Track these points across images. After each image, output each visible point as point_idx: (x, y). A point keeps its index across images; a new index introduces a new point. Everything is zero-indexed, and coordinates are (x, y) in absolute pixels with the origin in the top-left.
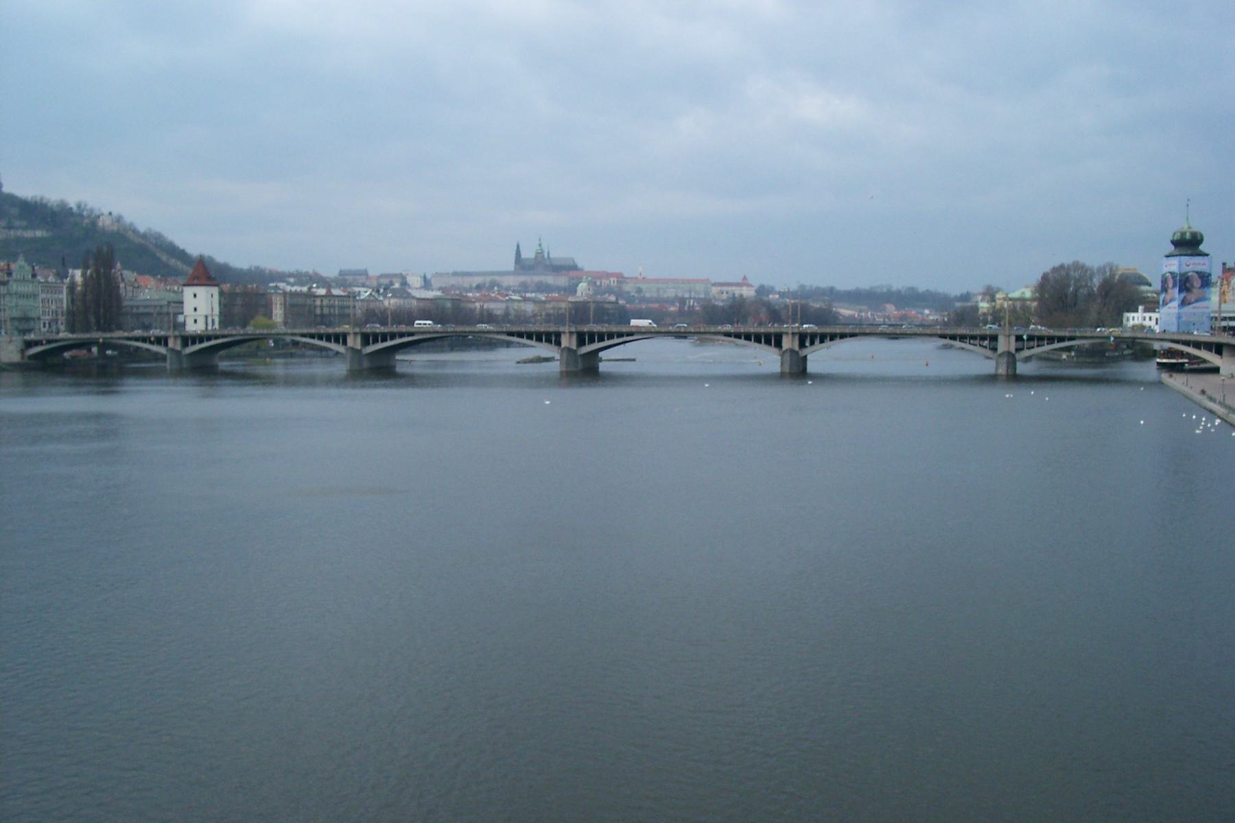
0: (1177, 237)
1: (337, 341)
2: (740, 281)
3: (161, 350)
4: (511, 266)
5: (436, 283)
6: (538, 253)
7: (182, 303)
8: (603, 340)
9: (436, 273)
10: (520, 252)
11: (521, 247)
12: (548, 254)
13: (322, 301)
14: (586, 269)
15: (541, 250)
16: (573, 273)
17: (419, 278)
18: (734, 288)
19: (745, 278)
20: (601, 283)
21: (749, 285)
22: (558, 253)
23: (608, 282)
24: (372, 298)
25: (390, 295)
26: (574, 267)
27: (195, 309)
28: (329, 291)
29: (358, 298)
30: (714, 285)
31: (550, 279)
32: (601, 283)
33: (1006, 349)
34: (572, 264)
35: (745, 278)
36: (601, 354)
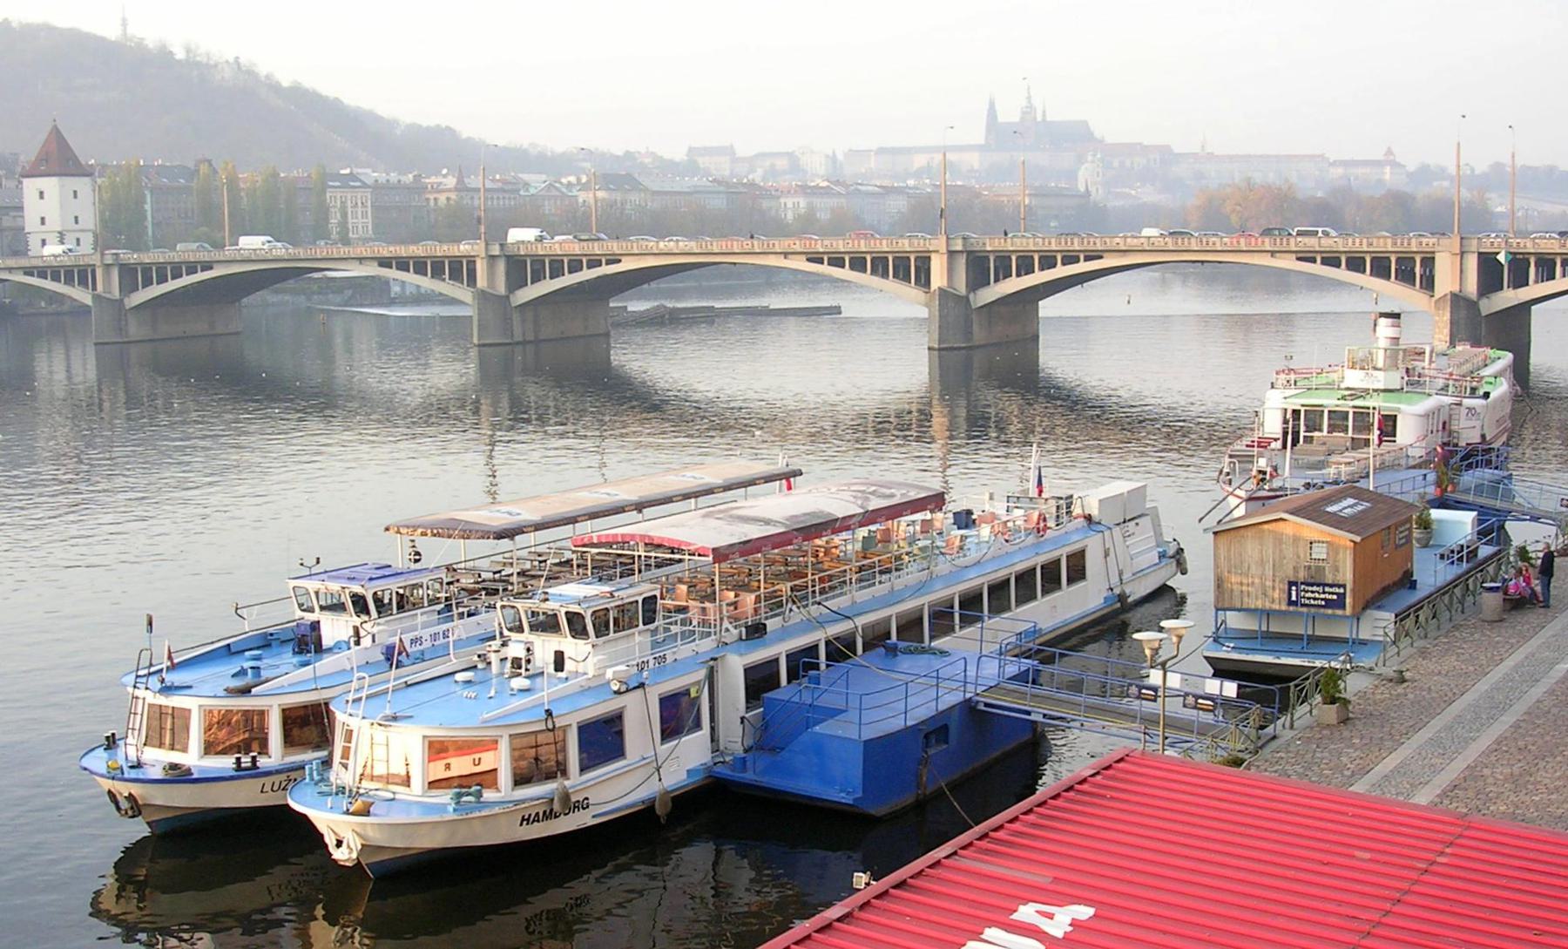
2: (1379, 155)
3: (83, 296)
4: (979, 137)
7: (21, 208)
9: (850, 150)
10: (995, 111)
11: (998, 107)
12: (1044, 112)
14: (1109, 140)
15: (1031, 107)
19: (1389, 152)
20: (1132, 163)
21: (1395, 165)
22: (1059, 111)
27: (43, 221)
28: (460, 181)
29: (522, 193)
30: (1334, 164)
32: (1132, 163)
33: (1456, 289)
35: (1389, 152)
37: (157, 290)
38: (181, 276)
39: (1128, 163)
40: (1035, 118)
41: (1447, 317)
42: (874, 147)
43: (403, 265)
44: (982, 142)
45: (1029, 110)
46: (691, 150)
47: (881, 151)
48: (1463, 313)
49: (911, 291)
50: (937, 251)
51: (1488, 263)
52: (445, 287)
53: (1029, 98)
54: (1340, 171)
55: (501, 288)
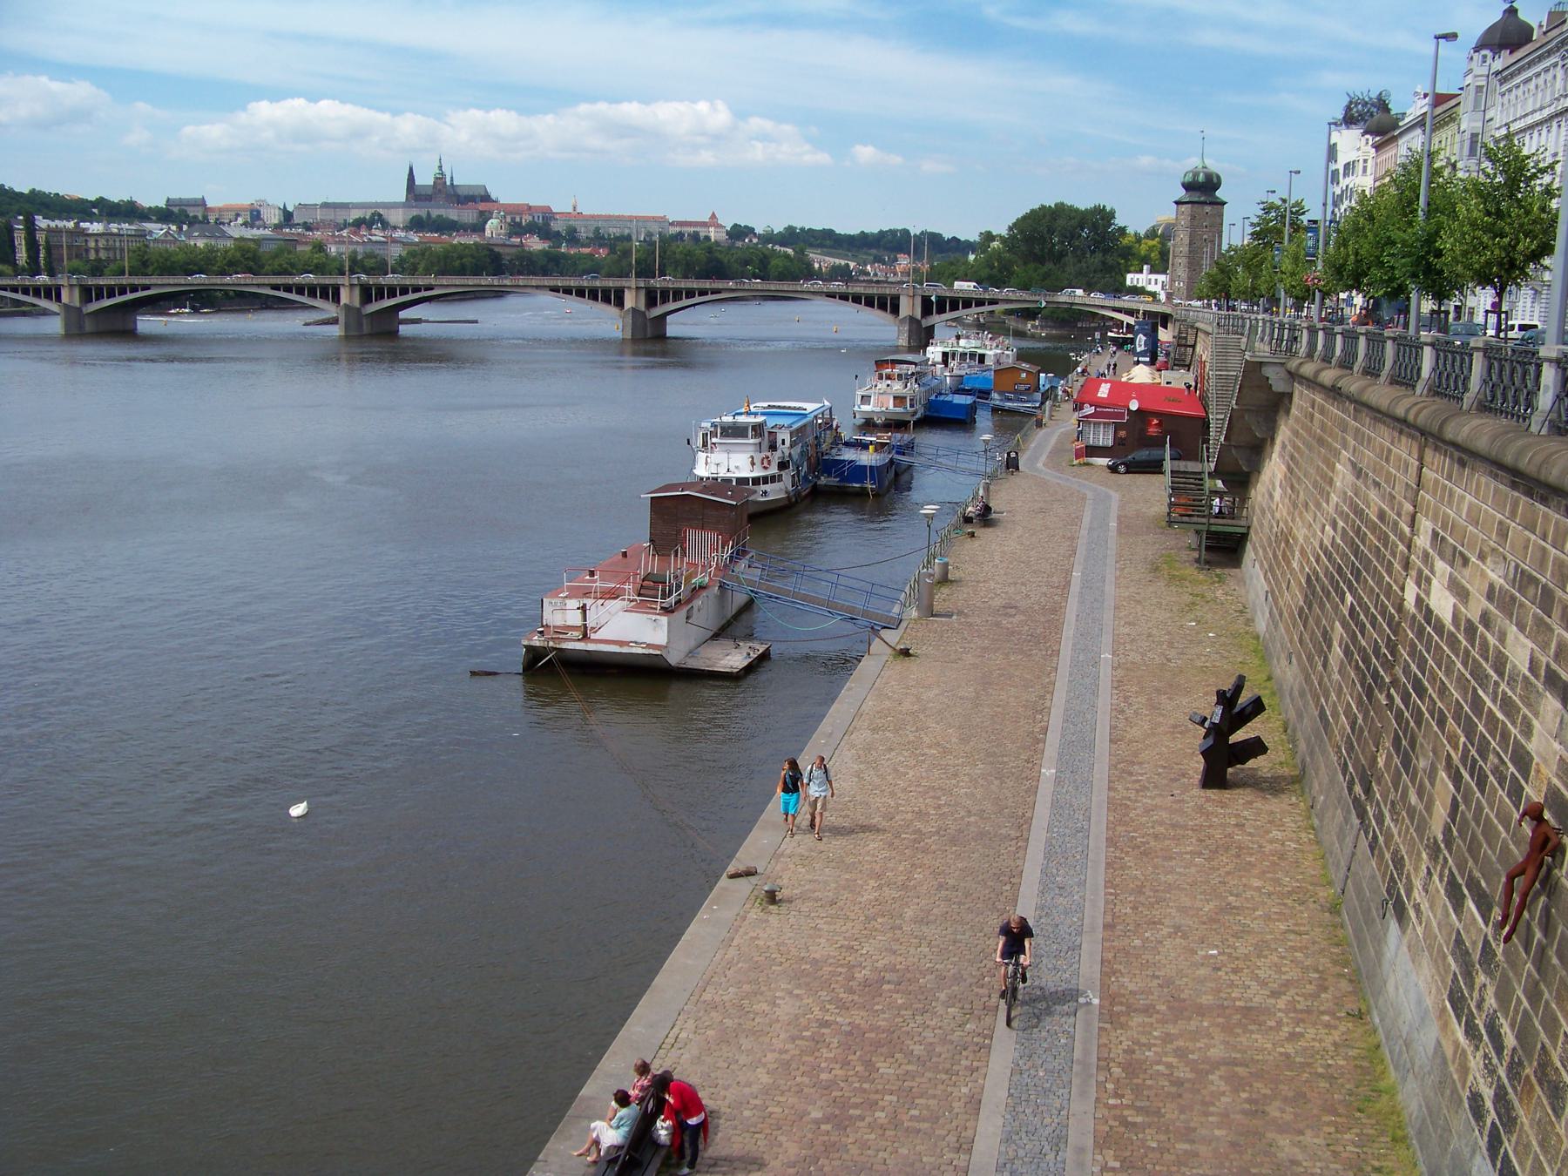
0: (1189, 178)
1: (48, 296)
2: (706, 219)
4: (401, 196)
5: (297, 219)
6: (437, 178)
8: (395, 296)
12: (452, 178)
13: (97, 241)
14: (502, 201)
16: (482, 206)
17: (277, 212)
18: (698, 229)
19: (713, 216)
22: (463, 178)
23: (531, 218)
24: (170, 238)
25: (196, 234)
26: (486, 198)
30: (672, 224)
31: (453, 214)
34: (483, 193)
35: (713, 216)
36: (403, 314)
37: (107, 303)
38: (126, 293)
39: (518, 220)
40: (445, 183)
41: (907, 328)
42: (319, 202)
43: (288, 289)
44: (404, 200)
45: (440, 179)
46: (168, 200)
47: (325, 205)
48: (914, 326)
49: (612, 310)
50: (629, 288)
51: (926, 303)
52: (318, 303)
53: (440, 167)
54: (678, 229)
55: (357, 303)
